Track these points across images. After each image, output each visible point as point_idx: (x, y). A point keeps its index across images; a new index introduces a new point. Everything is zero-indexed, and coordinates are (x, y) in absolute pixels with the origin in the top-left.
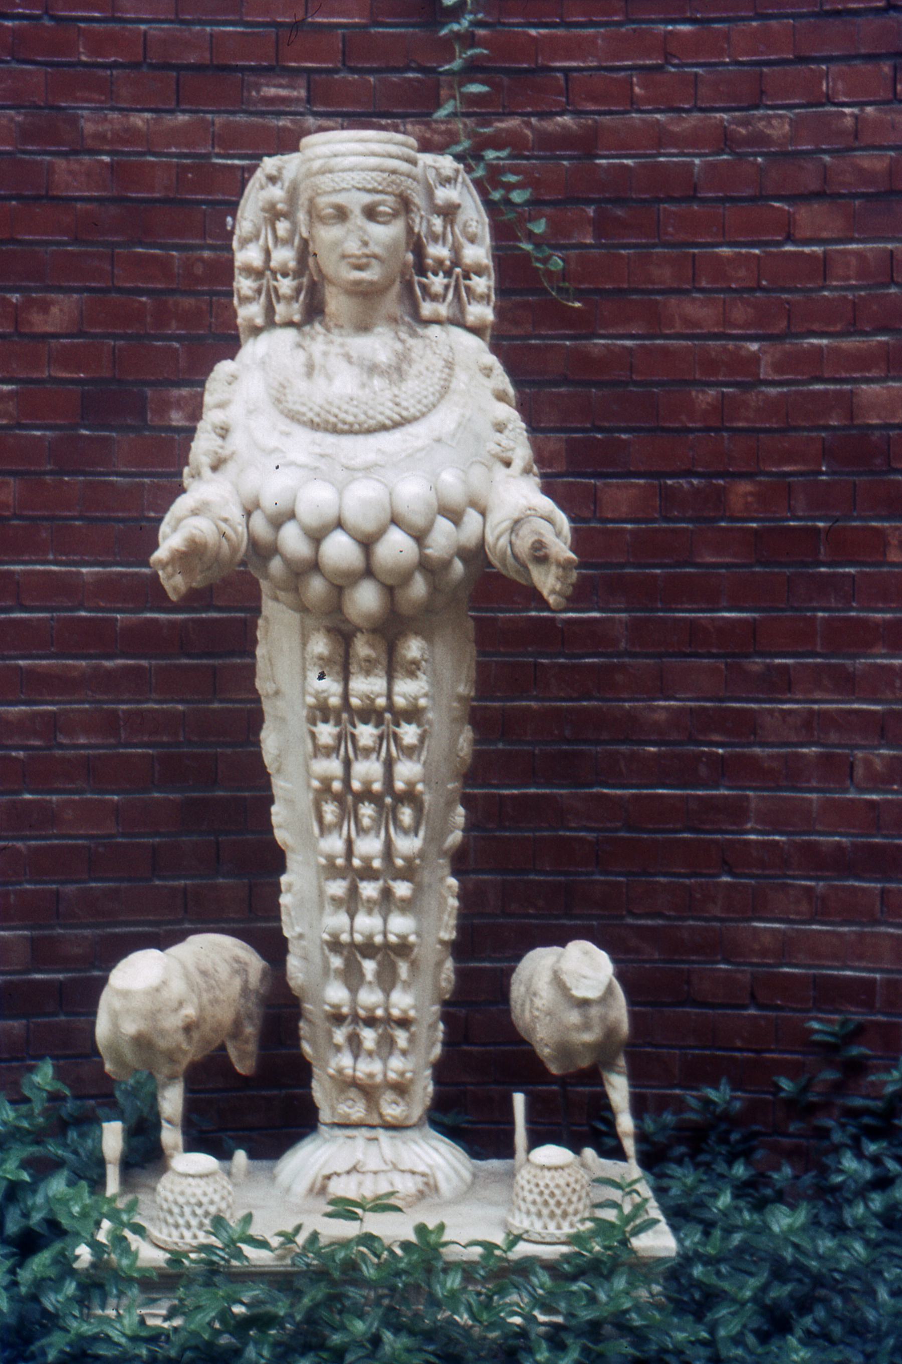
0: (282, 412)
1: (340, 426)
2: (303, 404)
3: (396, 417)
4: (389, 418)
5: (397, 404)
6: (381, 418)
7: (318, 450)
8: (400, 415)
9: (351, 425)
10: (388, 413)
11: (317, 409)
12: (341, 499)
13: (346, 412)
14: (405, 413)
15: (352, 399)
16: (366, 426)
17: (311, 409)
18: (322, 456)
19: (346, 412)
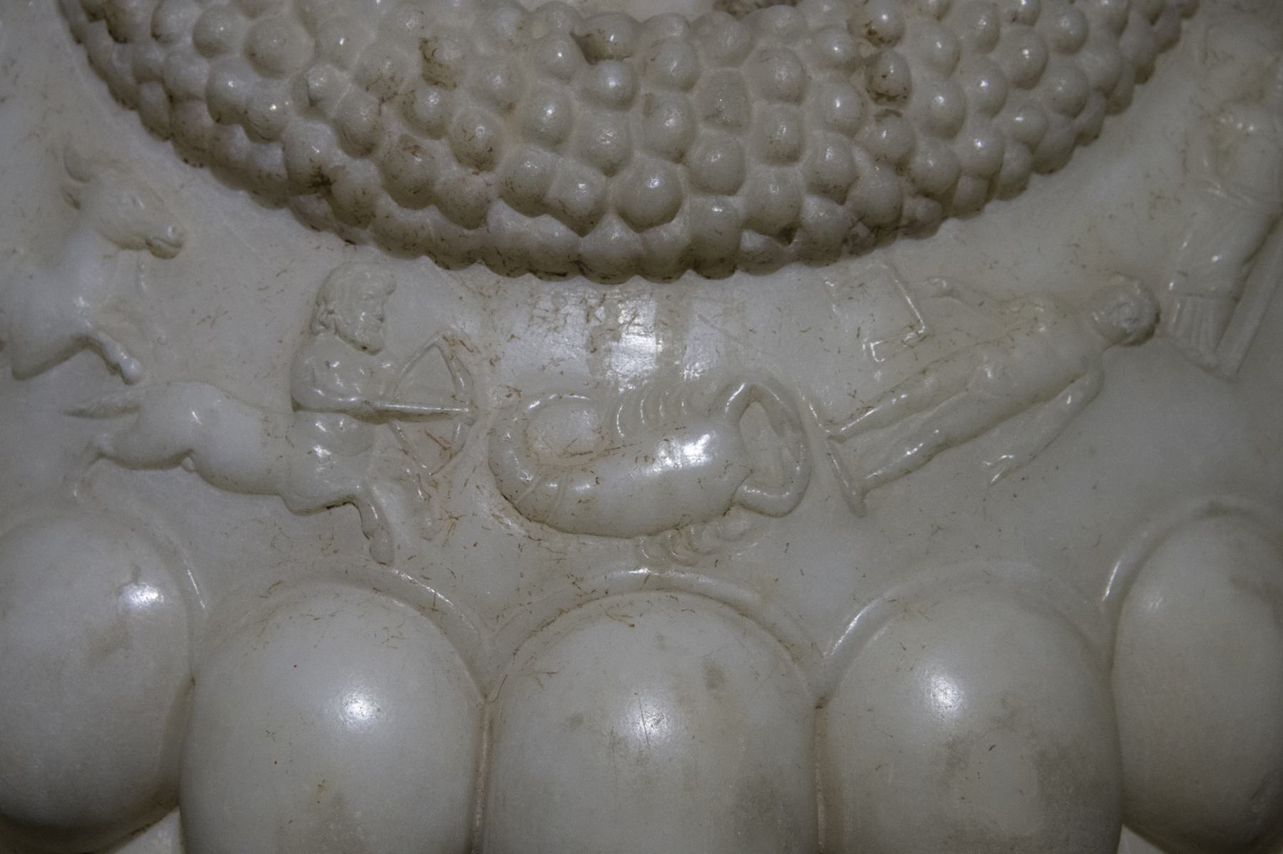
0: (125, 98)
1: (509, 222)
2: (262, 63)
3: (876, 187)
4: (835, 192)
5: (890, 99)
6: (770, 185)
7: (347, 382)
8: (900, 166)
9: (584, 223)
10: (828, 155)
11: (364, 114)
12: (490, 726)
13: (555, 141)
14: (928, 161)
15: (591, 51)
16: (676, 232)
17: (313, 105)
18: (382, 416)
19: (555, 141)
